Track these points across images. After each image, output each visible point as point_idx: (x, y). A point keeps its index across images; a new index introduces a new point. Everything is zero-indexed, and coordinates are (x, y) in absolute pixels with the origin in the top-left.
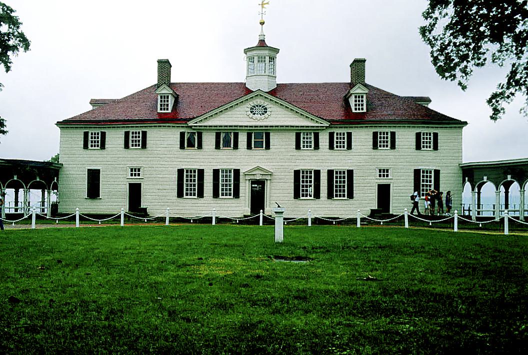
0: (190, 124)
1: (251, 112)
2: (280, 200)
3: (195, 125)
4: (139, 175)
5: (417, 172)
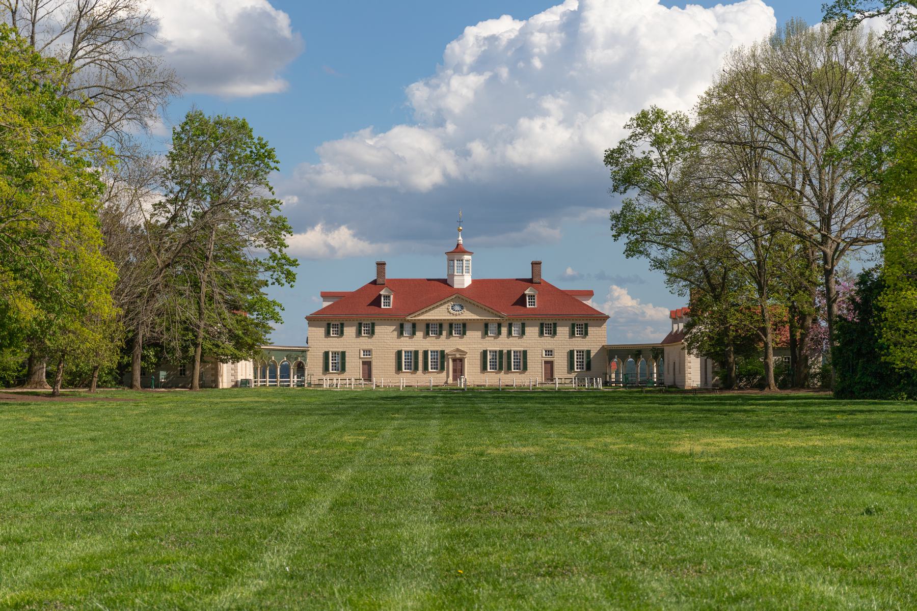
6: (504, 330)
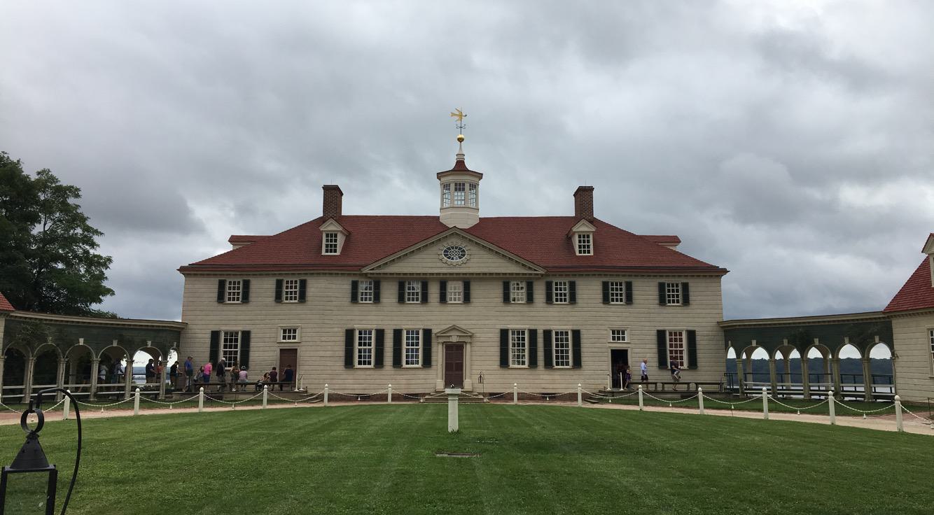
0: (366, 270)
1: (445, 255)
2: (483, 372)
3: (371, 272)
4: (294, 337)
5: (661, 335)
6: (540, 293)
